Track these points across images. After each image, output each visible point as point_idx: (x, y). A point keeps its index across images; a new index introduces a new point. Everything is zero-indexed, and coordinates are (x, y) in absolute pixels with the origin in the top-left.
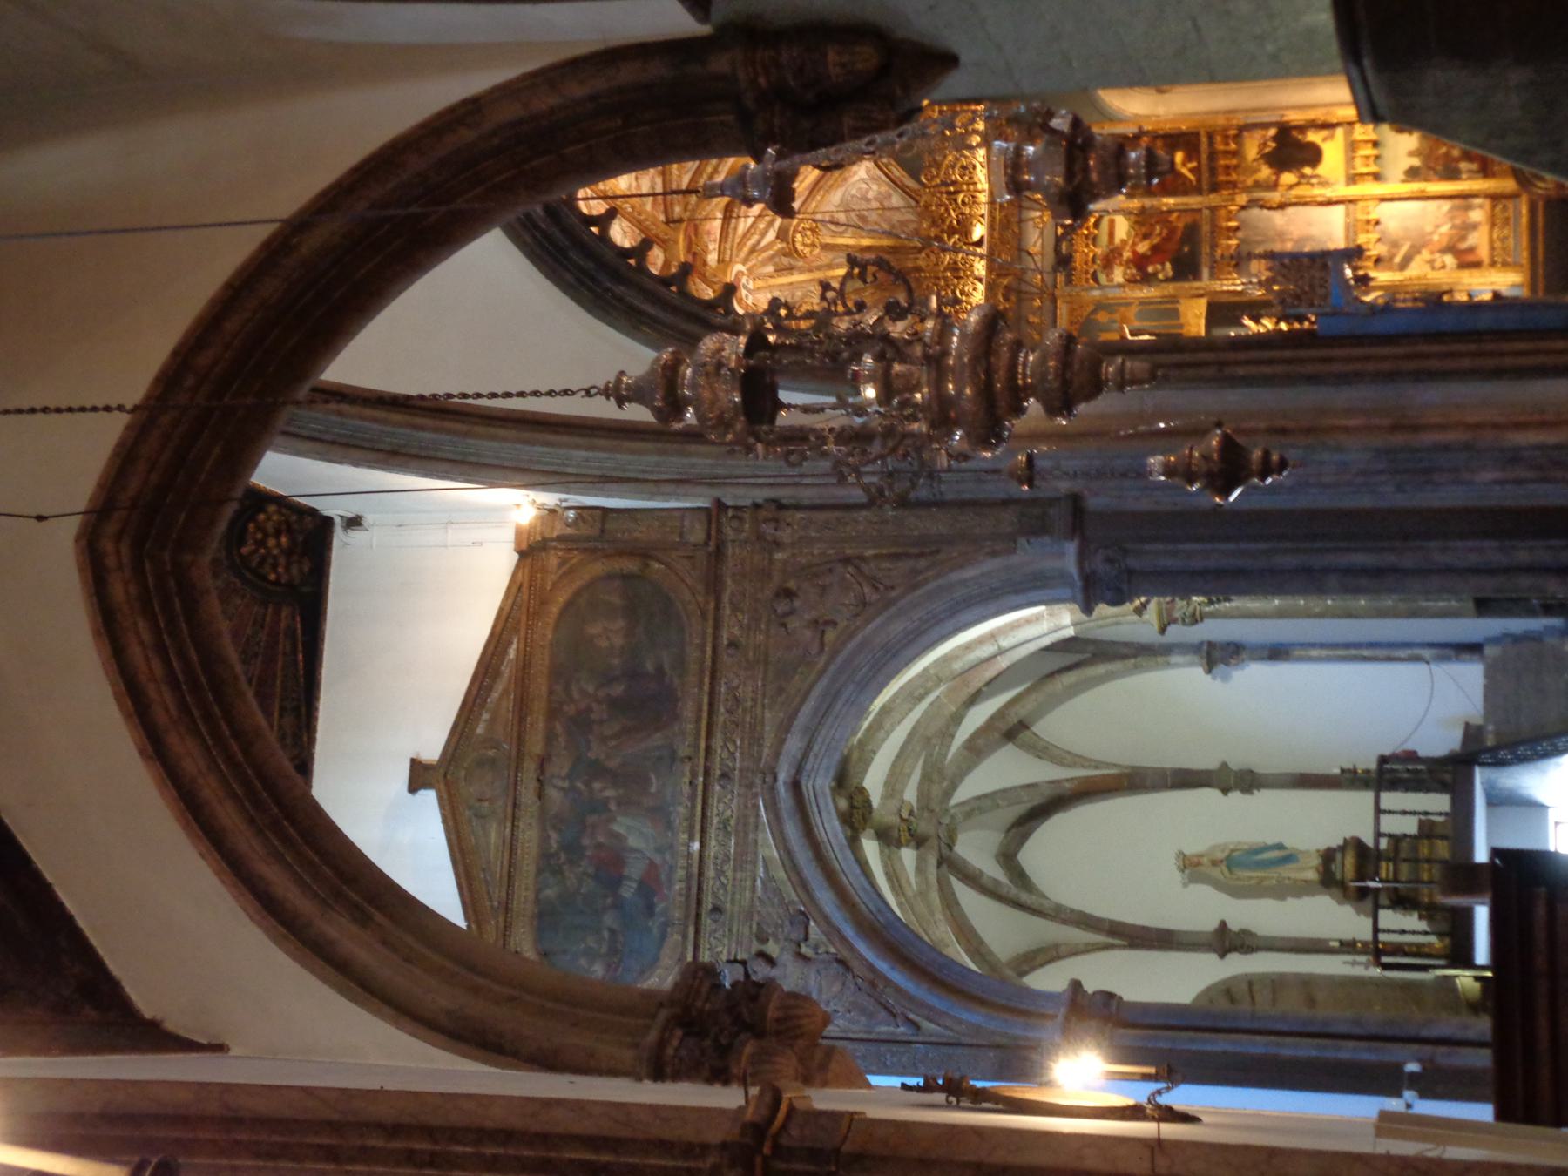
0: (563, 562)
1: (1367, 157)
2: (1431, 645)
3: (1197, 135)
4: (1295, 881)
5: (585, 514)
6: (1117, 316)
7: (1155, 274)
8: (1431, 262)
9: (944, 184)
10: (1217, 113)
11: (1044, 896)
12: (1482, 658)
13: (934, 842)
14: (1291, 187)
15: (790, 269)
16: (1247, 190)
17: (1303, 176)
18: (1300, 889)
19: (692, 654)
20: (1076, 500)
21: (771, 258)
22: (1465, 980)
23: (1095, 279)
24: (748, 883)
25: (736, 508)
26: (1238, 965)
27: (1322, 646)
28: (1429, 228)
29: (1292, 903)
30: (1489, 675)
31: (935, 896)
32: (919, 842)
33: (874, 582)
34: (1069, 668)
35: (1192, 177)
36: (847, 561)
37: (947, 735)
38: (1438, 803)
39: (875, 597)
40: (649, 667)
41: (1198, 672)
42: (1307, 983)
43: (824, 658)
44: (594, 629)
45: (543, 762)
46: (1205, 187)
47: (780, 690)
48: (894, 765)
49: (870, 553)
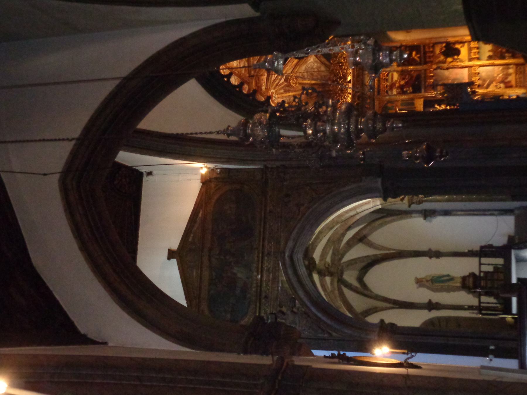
1: (475, 52)
2: (496, 210)
4: (453, 287)
6: (394, 105)
7: (406, 91)
10: (426, 39)
11: (371, 292)
12: (514, 214)
15: (289, 91)
17: (454, 59)
22: (509, 318)
23: (387, 92)
25: (272, 168)
26: (435, 314)
27: (462, 211)
28: (495, 75)
31: (336, 292)
32: (331, 274)
34: (379, 218)
35: (418, 60)
37: (340, 240)
38: (500, 261)
42: (457, 319)
43: (300, 216)
48: (323, 250)
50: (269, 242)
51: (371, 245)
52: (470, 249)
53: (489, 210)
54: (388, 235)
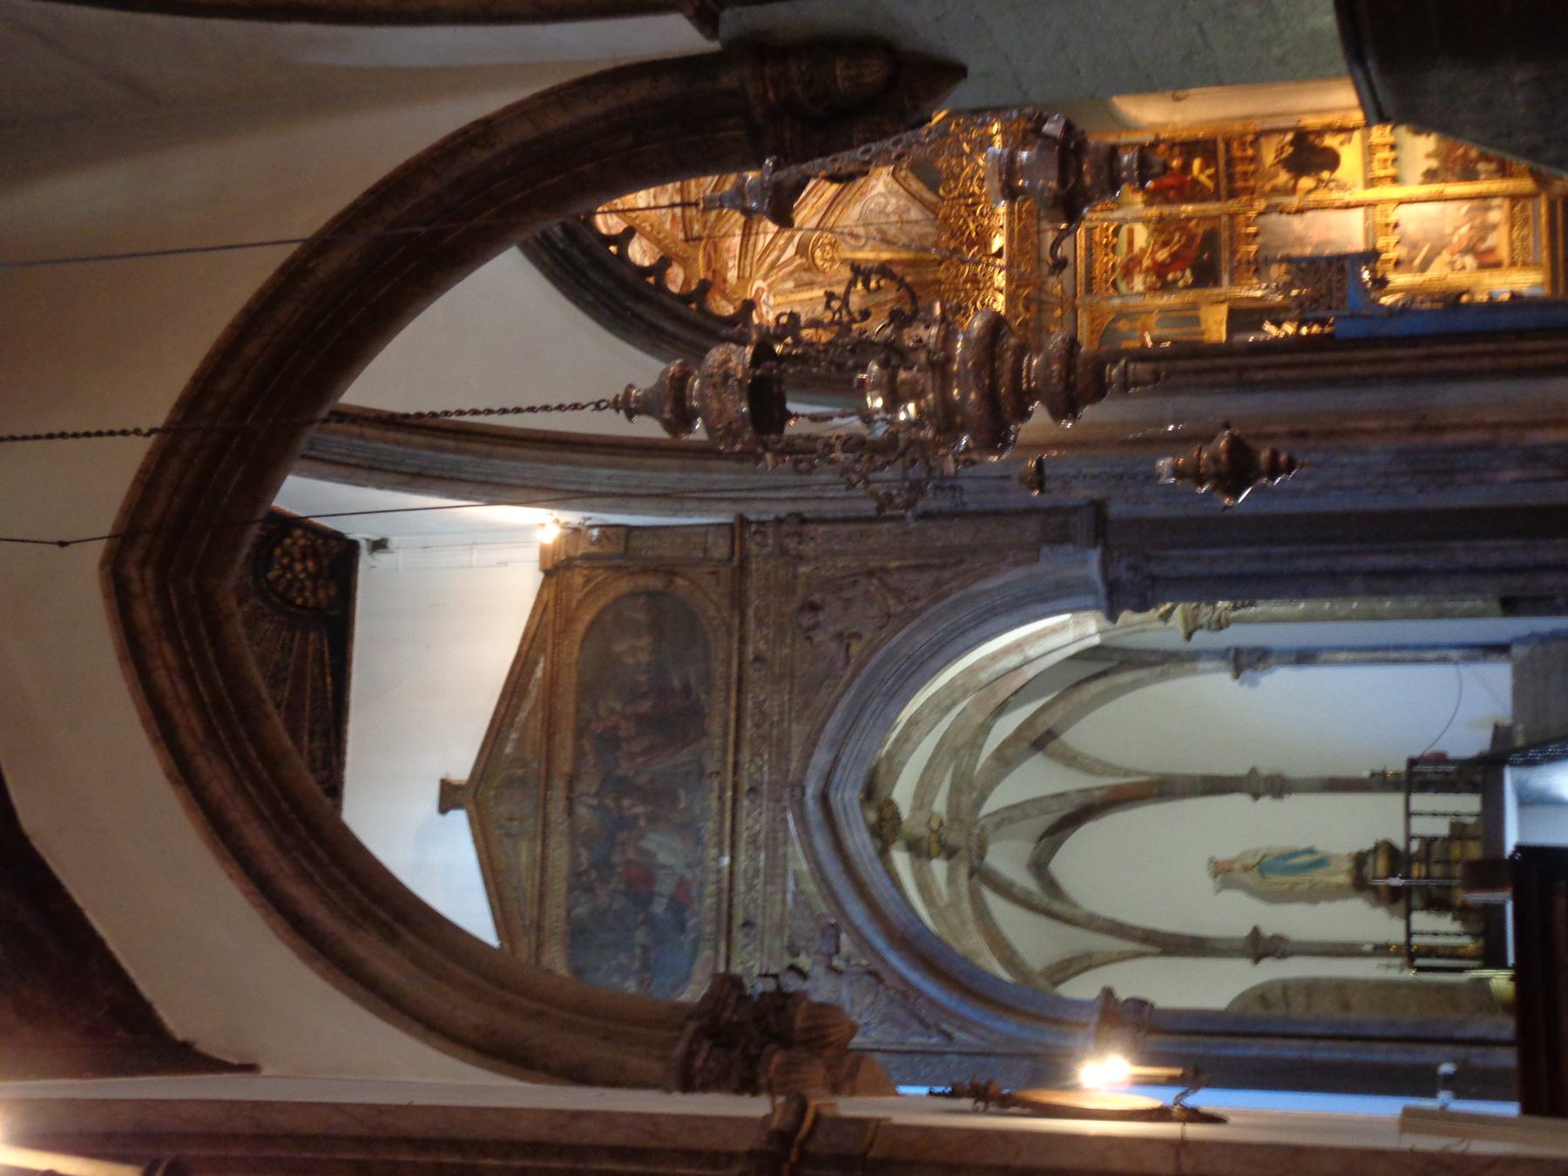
0: (588, 581)
1: (1385, 160)
3: (1214, 142)
5: (609, 532)
6: (1138, 324)
7: (1175, 281)
8: (1452, 264)
9: (960, 196)
10: (1234, 119)
11: (1075, 905)
12: (1510, 658)
13: (963, 853)
14: (1310, 191)
15: (811, 285)
16: (1265, 195)
17: (1320, 181)
18: (1332, 893)
19: (718, 668)
20: (1098, 508)
21: (791, 273)
24: (779, 897)
25: (762, 523)
27: (1351, 649)
29: (1324, 907)
30: (1518, 674)
31: (966, 906)
32: (950, 853)
33: (898, 594)
35: (1209, 184)
36: (870, 573)
37: (975, 744)
38: (1468, 804)
39: (900, 608)
40: (676, 683)
42: (1341, 987)
44: (620, 647)
45: (572, 780)
46: (1223, 193)
47: (806, 705)
48: (923, 776)
49: (894, 564)
50: (756, 754)
52: (1379, 769)
53: (1435, 647)
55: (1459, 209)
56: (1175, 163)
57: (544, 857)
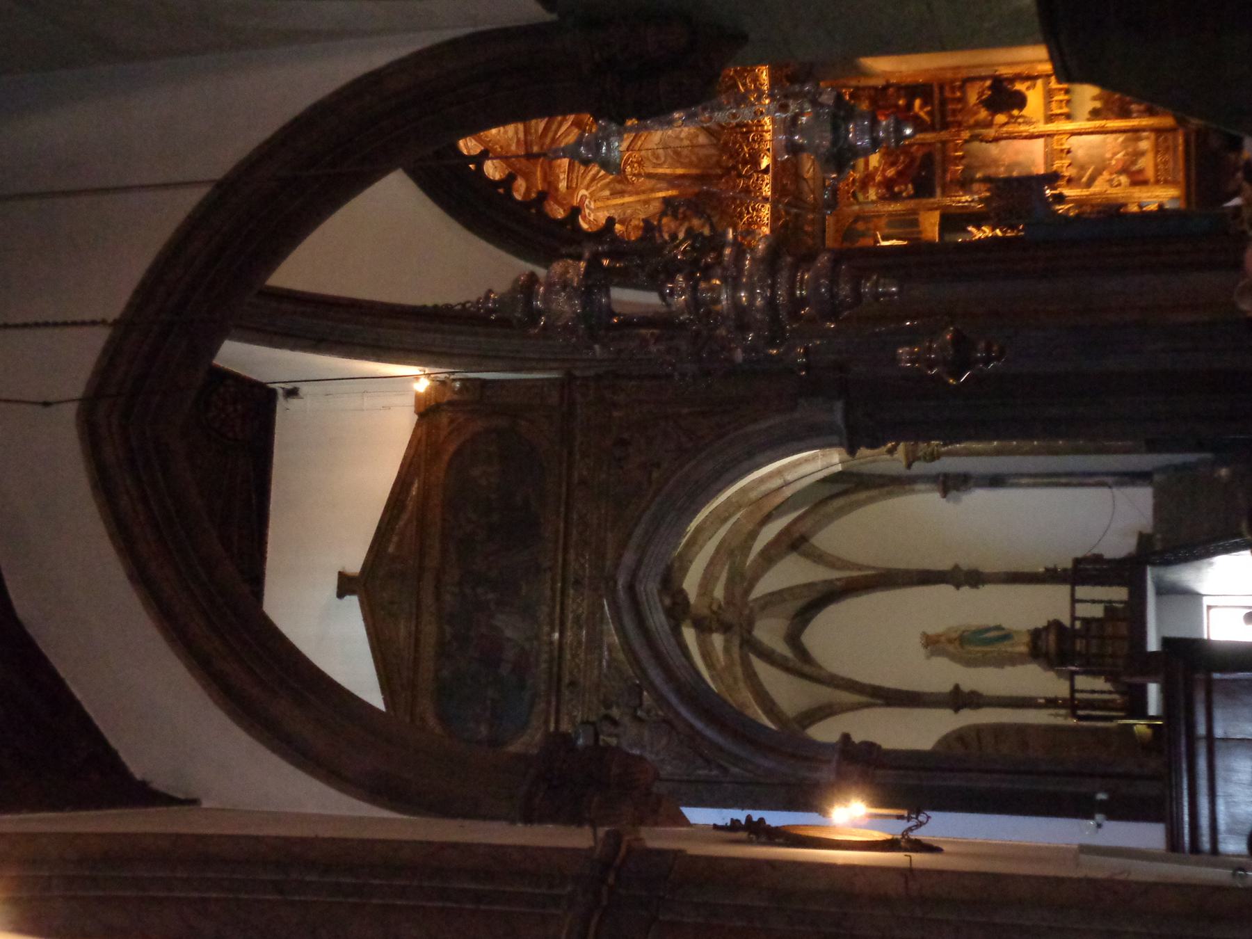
0: (452, 421)
6: (871, 226)
7: (900, 193)
11: (820, 668)
15: (622, 193)
16: (970, 127)
17: (1012, 117)
18: (1013, 660)
22: (1140, 727)
25: (586, 378)
28: (1108, 155)
29: (1009, 670)
31: (739, 670)
32: (726, 628)
38: (1119, 594)
41: (936, 496)
46: (938, 126)
49: (685, 411)
51: (819, 558)
52: (1051, 566)
54: (861, 533)
55: (1116, 139)
56: (901, 102)
57: (418, 631)
